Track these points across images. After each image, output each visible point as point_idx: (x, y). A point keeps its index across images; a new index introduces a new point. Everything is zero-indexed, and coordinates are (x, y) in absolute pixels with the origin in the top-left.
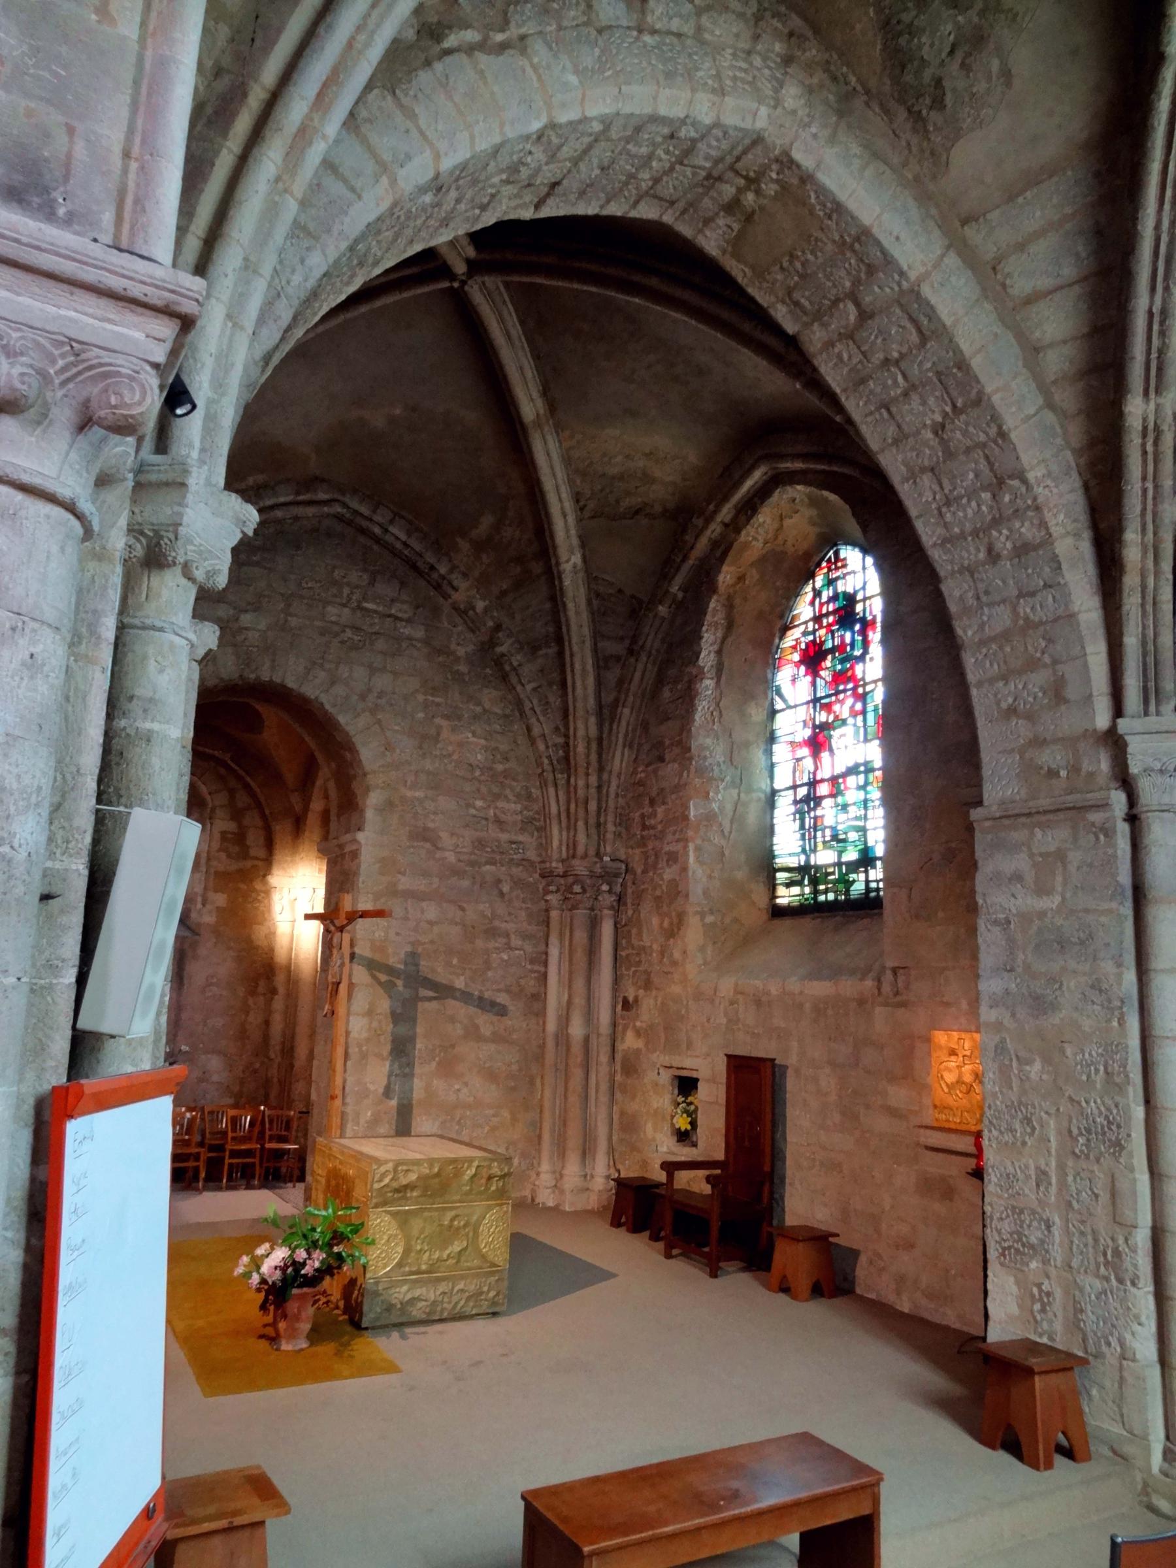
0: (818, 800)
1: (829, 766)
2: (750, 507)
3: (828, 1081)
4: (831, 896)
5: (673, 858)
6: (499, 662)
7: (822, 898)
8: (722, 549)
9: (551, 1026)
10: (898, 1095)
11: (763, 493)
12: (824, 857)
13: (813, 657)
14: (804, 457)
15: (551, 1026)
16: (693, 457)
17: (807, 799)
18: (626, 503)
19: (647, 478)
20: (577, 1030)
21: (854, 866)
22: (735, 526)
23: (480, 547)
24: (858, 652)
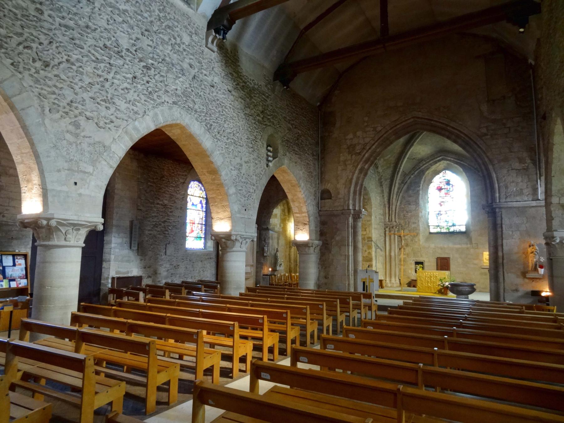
0: (441, 215)
1: (443, 209)
2: (436, 162)
3: (460, 260)
4: (445, 231)
5: (414, 223)
6: (381, 183)
7: (442, 231)
8: (428, 169)
9: (387, 254)
10: (476, 262)
11: (439, 161)
12: (444, 224)
13: (440, 189)
14: (454, 158)
15: (387, 254)
16: (429, 152)
17: (438, 214)
18: (414, 157)
19: (420, 154)
20: (393, 254)
21: (451, 226)
22: (431, 165)
23: (385, 160)
24: (451, 190)
